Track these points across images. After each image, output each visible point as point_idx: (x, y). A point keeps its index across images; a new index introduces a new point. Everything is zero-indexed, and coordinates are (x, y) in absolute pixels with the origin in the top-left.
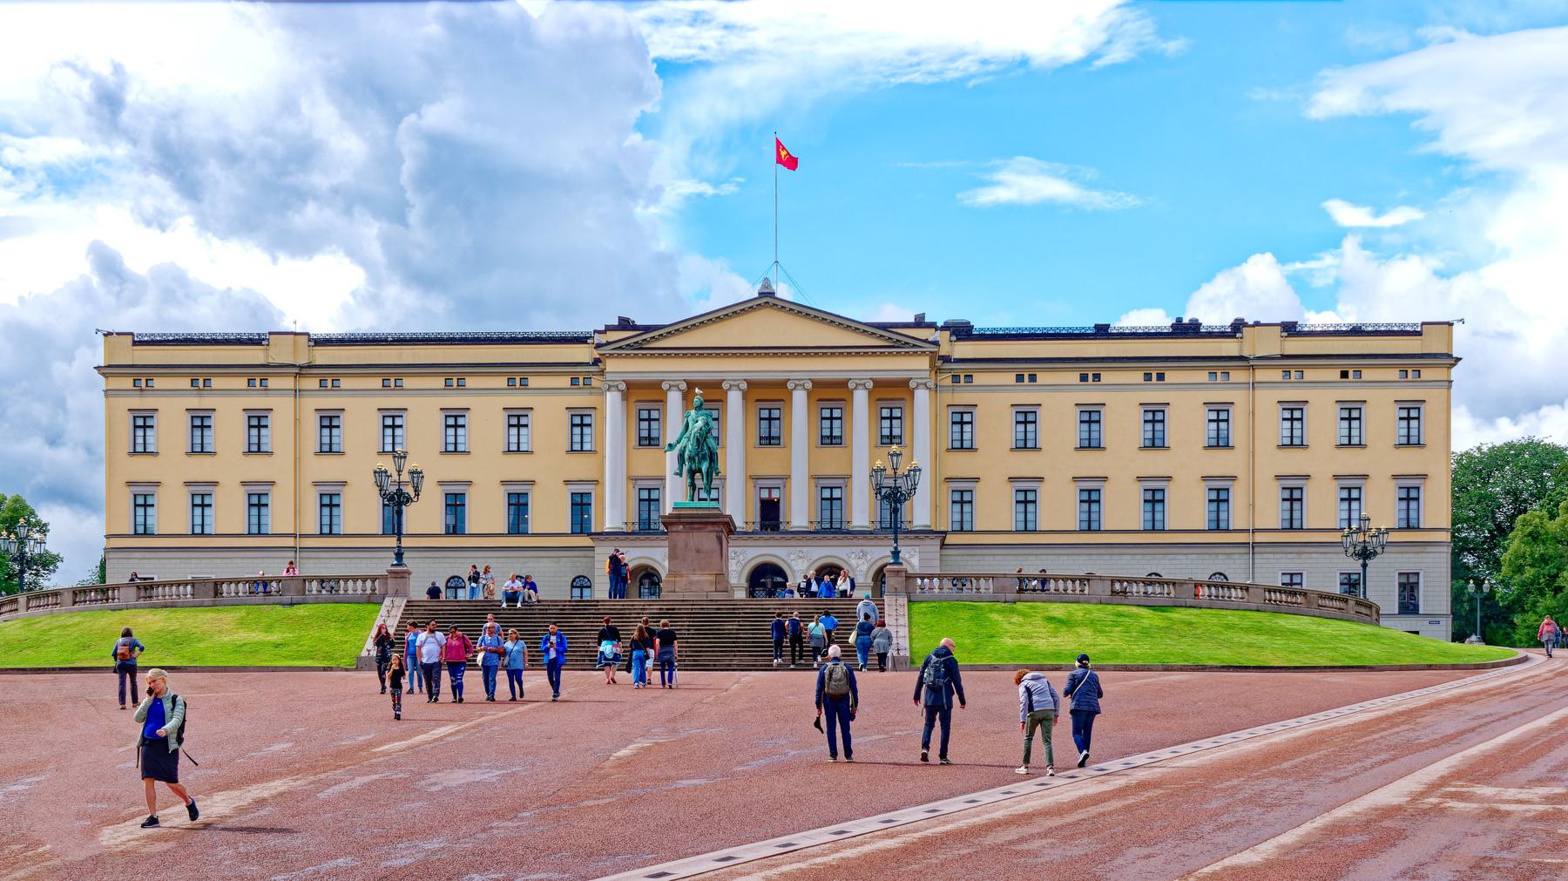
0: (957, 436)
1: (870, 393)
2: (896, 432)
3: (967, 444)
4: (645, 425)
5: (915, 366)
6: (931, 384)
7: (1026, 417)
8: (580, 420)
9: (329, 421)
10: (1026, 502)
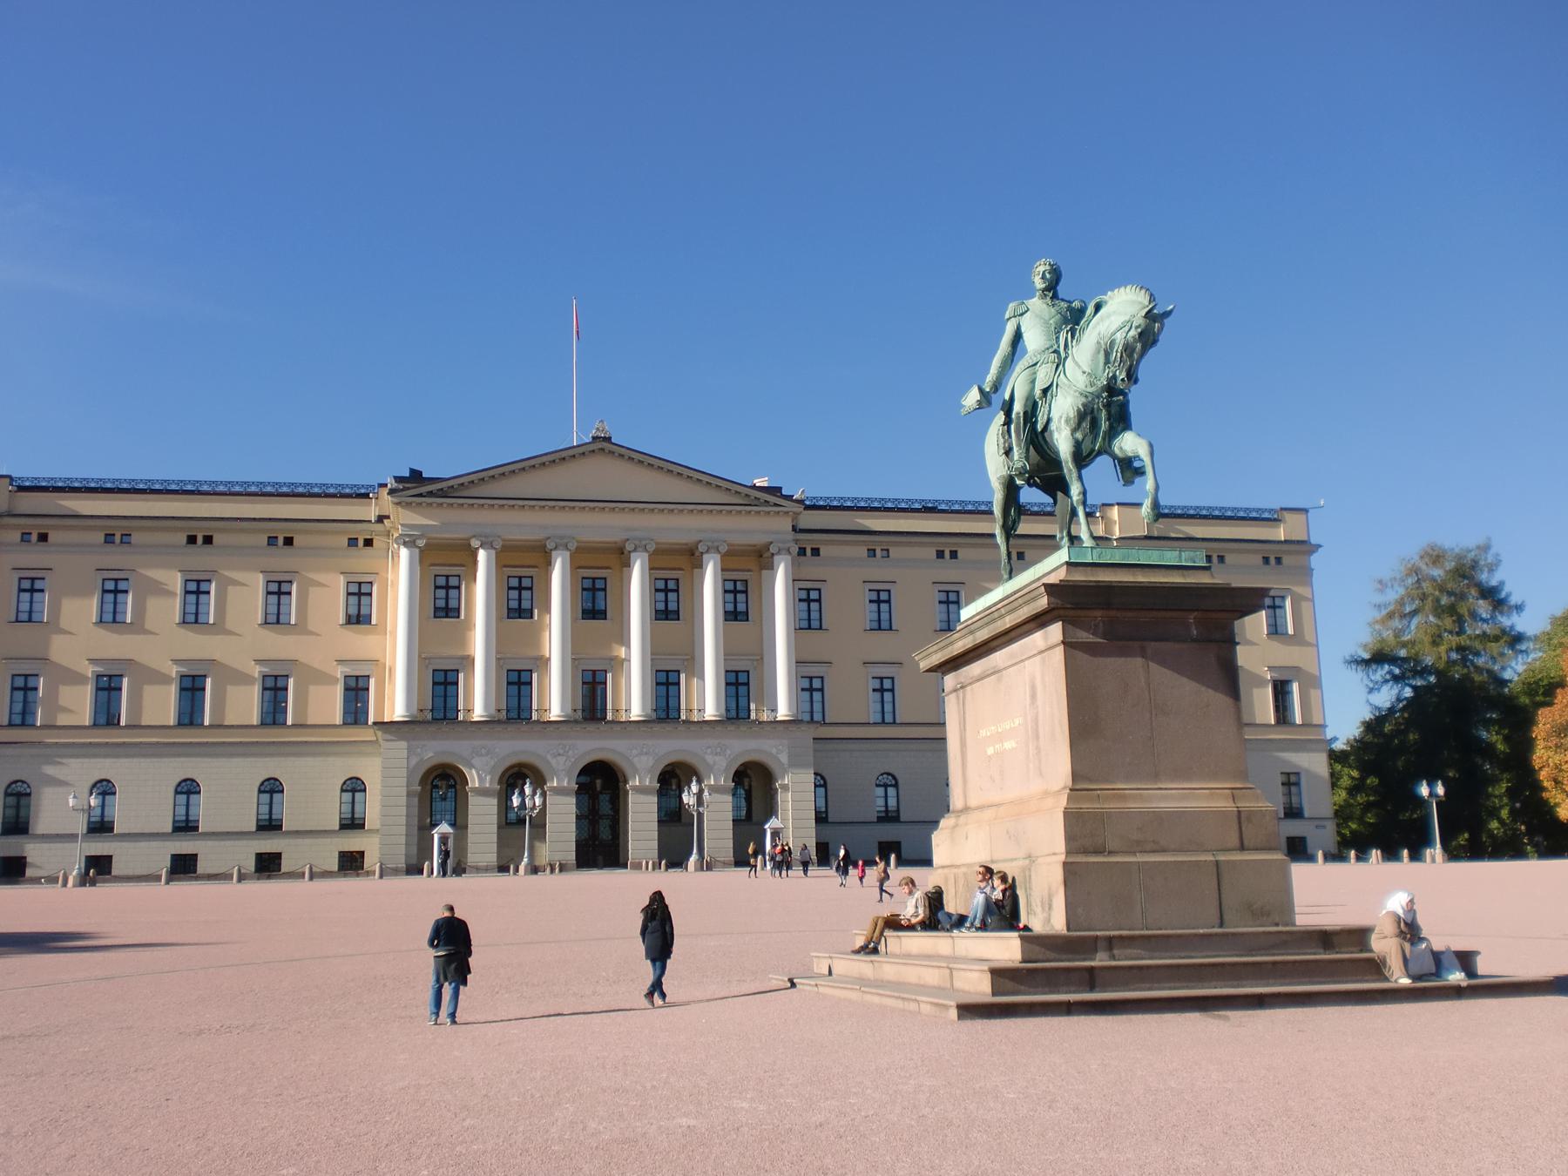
0: (805, 615)
1: (726, 556)
2: (741, 607)
3: (815, 624)
4: (441, 593)
5: (771, 527)
6: (795, 550)
7: (881, 599)
8: (360, 592)
10: (881, 690)
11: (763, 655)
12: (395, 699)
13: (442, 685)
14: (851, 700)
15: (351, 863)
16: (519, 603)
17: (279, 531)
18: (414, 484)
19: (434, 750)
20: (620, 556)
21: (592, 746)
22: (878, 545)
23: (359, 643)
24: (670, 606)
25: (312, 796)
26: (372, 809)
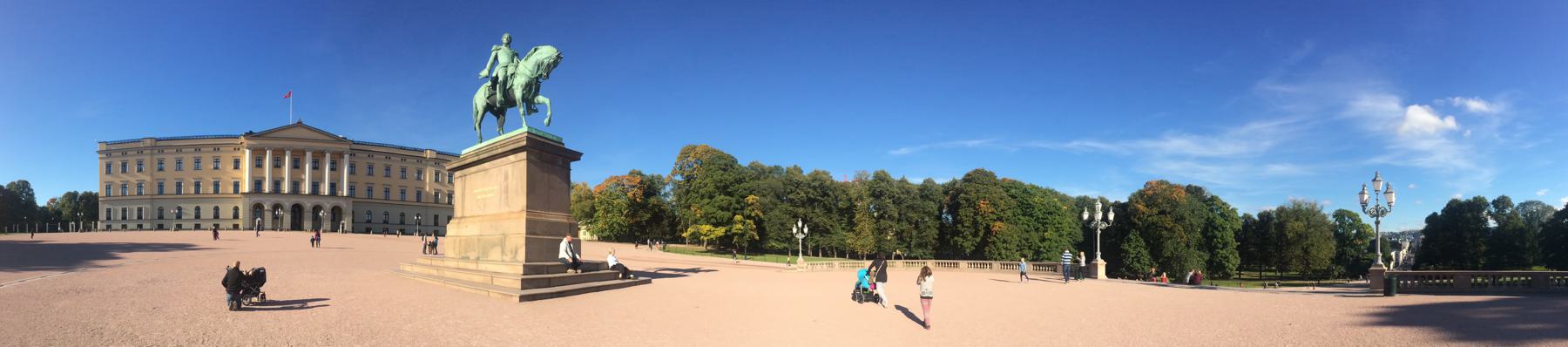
9: (161, 162)
11: (340, 179)
12: (246, 187)
13: (257, 184)
14: (361, 192)
15: (236, 227)
16: (277, 164)
17: (218, 144)
18: (250, 135)
19: (257, 199)
20: (303, 153)
21: (295, 200)
22: (371, 154)
23: (236, 173)
24: (316, 166)
25: (226, 211)
26: (241, 215)
